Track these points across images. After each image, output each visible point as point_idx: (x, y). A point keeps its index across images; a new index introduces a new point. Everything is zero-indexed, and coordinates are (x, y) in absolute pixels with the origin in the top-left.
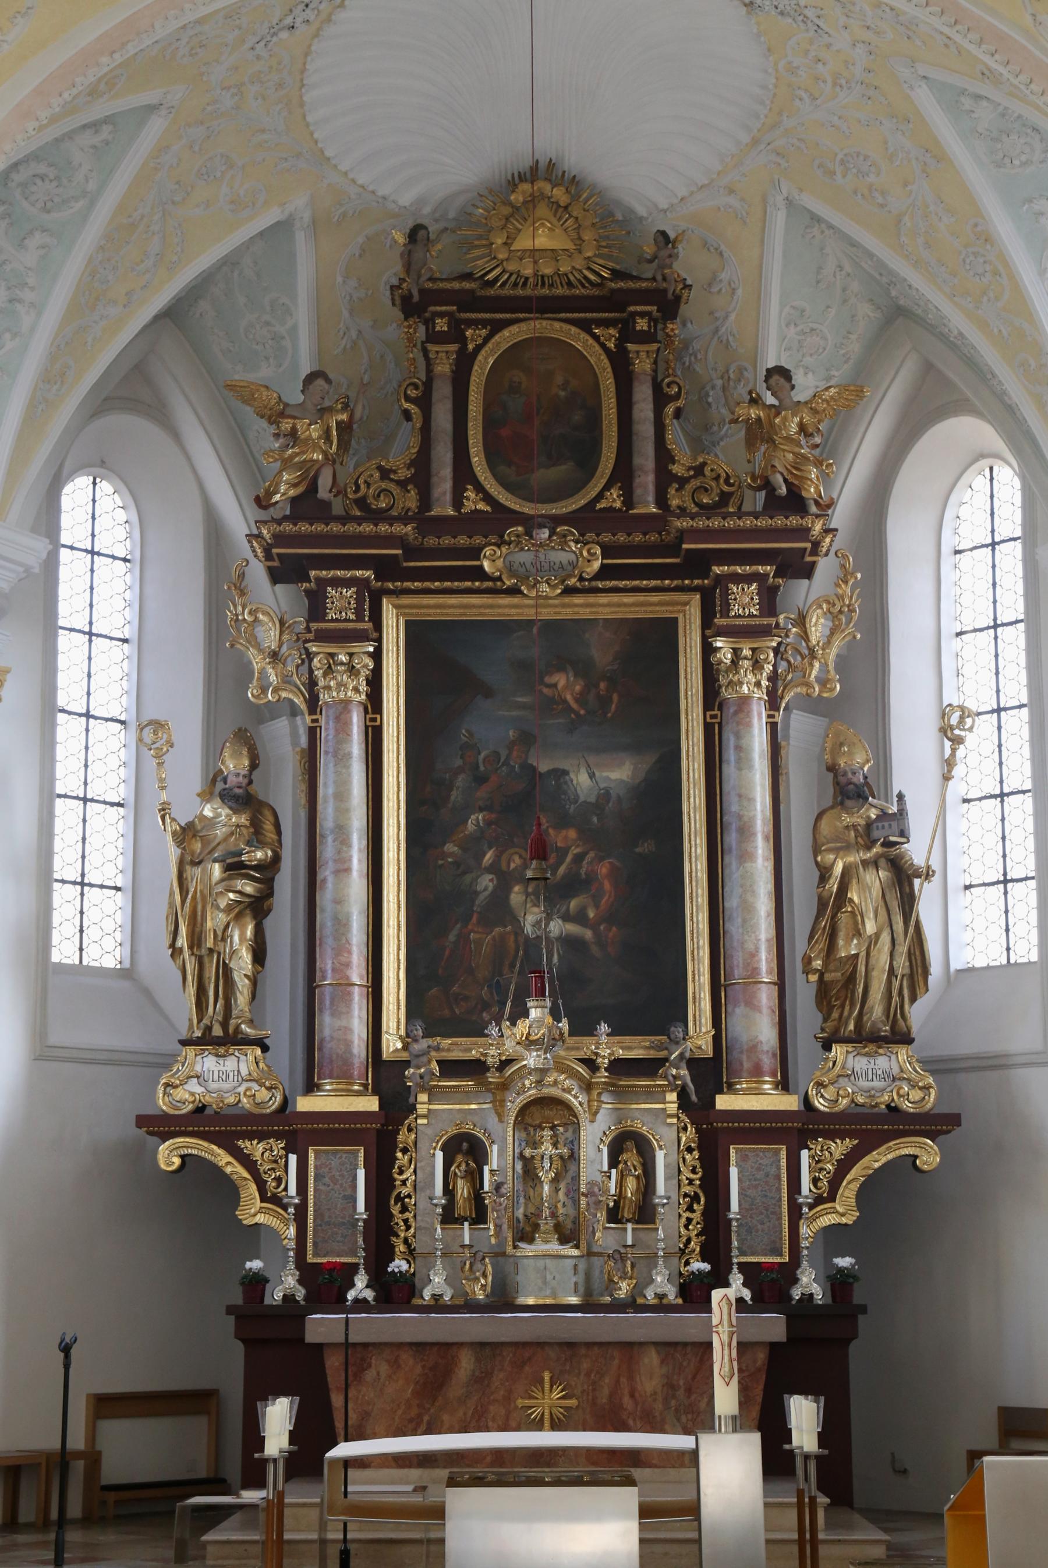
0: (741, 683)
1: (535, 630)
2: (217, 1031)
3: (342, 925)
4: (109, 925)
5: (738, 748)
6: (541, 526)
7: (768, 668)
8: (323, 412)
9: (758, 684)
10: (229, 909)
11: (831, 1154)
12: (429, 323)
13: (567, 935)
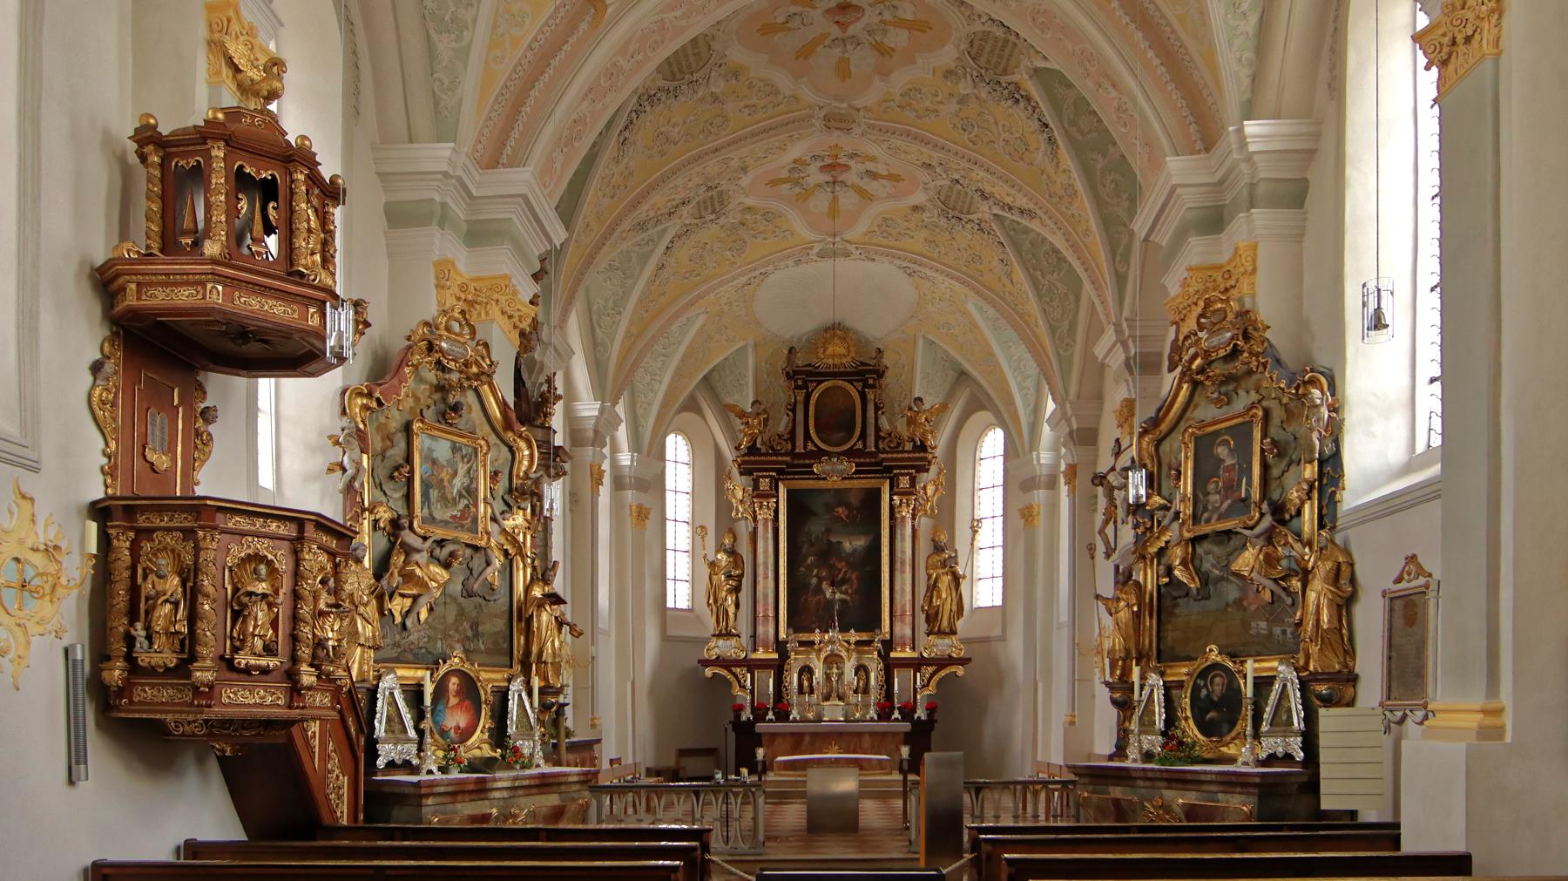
2: (724, 632)
3: (766, 596)
7: (912, 506)
8: (758, 414)
12: (796, 381)
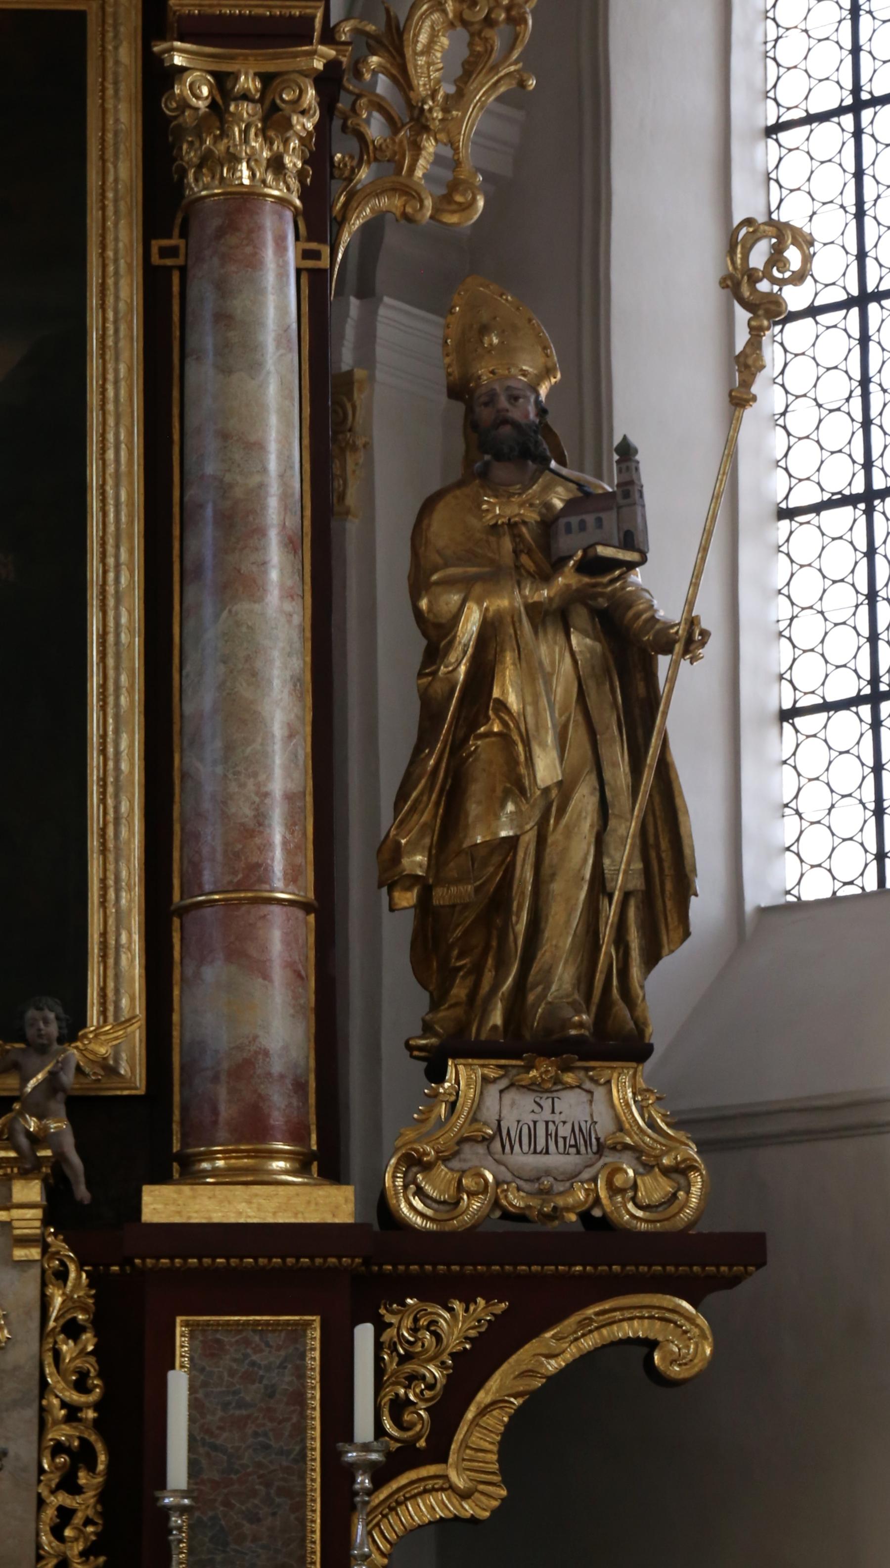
0: (233, 159)
5: (224, 318)
9: (276, 165)
11: (438, 1337)
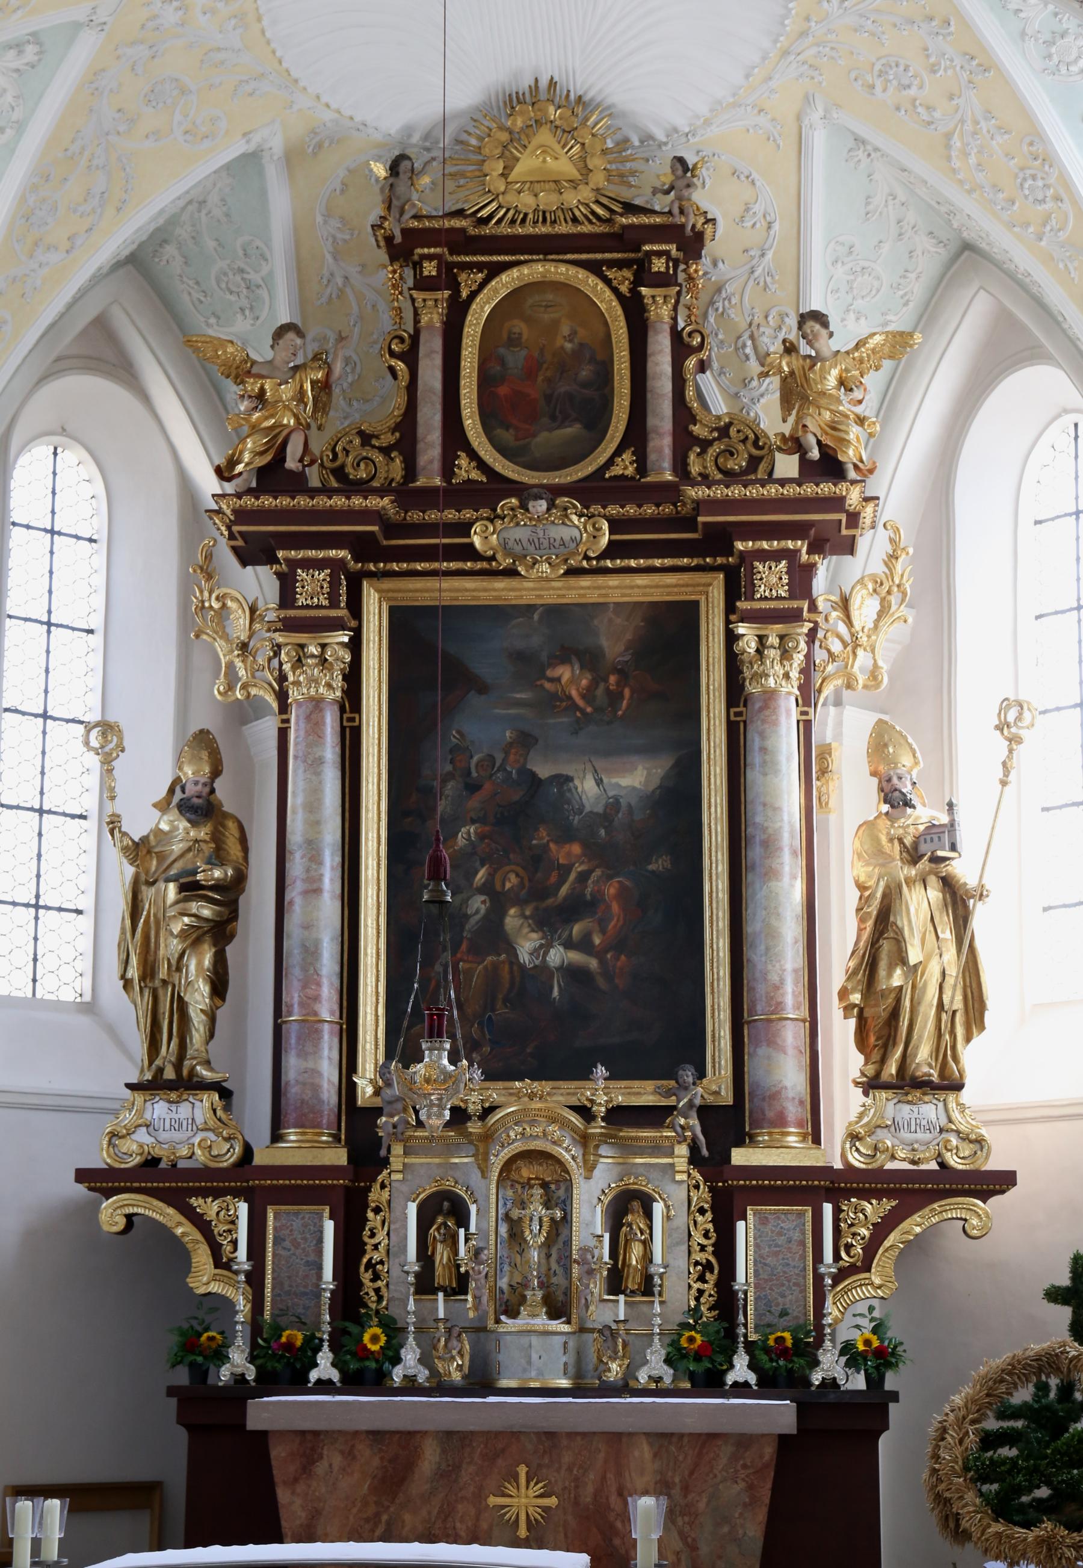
0: (767, 676)
1: (536, 617)
2: (169, 1074)
3: (311, 952)
4: (68, 954)
5: (764, 750)
6: (538, 497)
7: (799, 658)
9: (787, 676)
10: (183, 935)
11: (866, 1217)
12: (417, 266)
13: (569, 964)
